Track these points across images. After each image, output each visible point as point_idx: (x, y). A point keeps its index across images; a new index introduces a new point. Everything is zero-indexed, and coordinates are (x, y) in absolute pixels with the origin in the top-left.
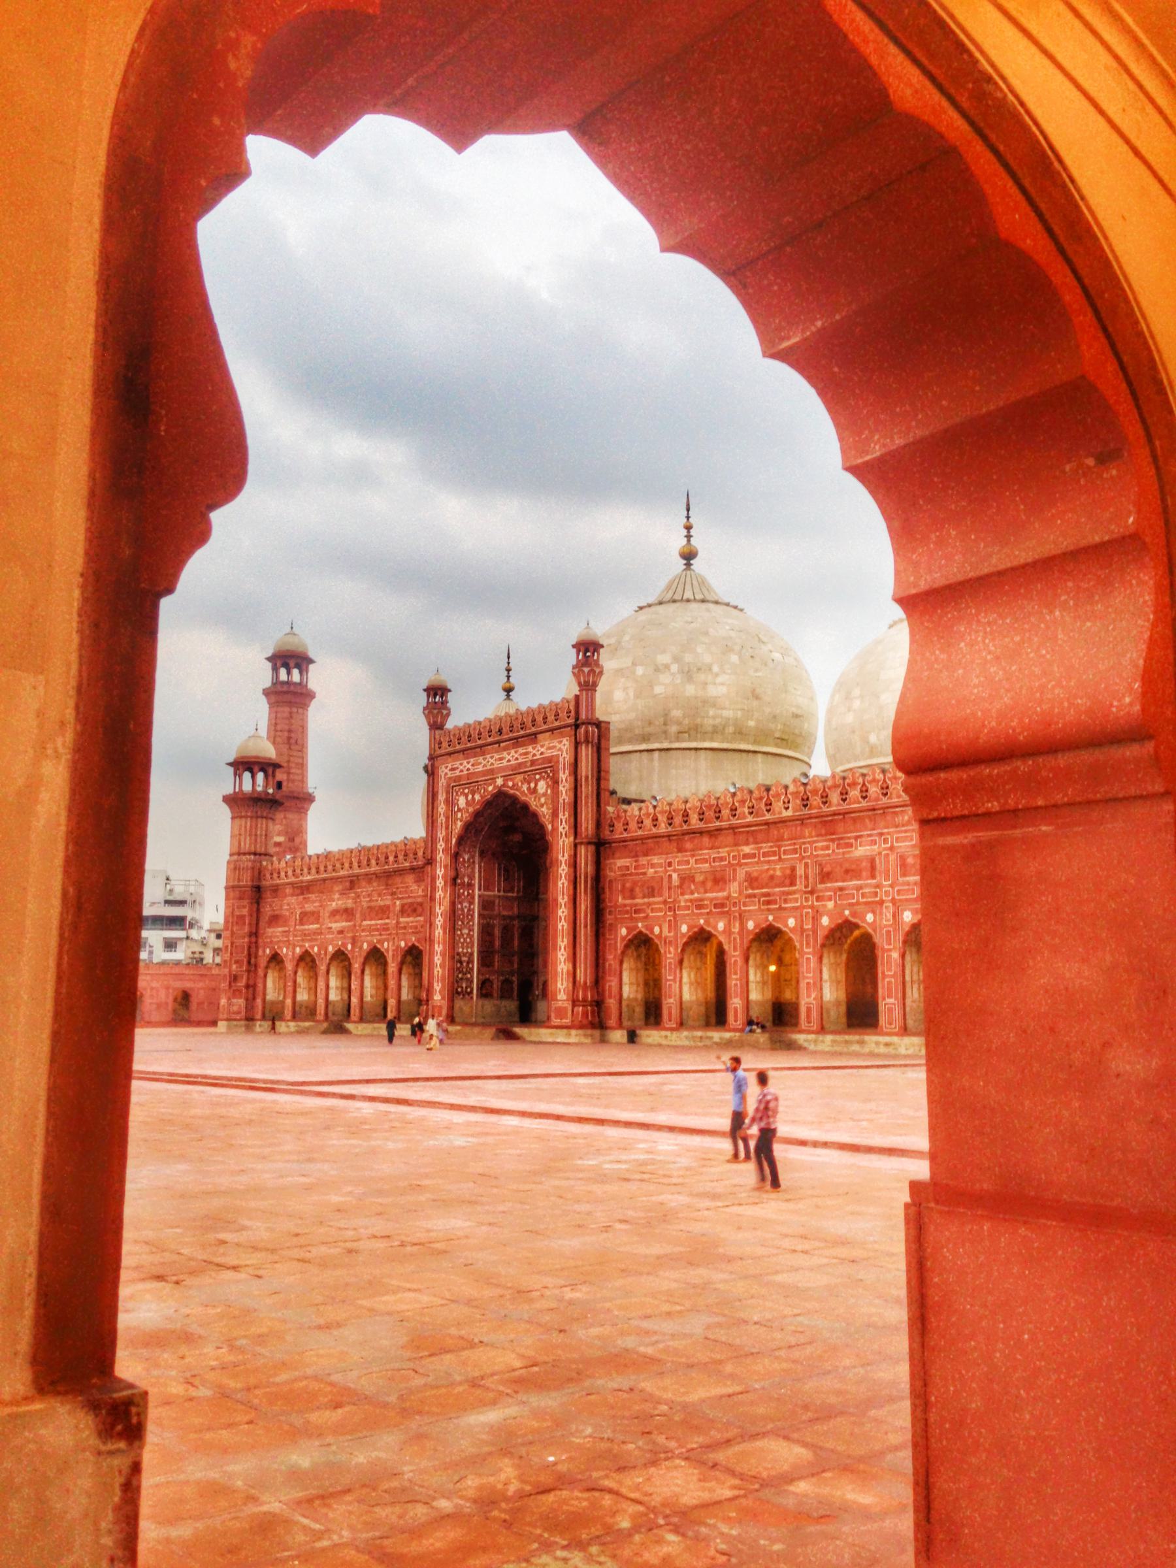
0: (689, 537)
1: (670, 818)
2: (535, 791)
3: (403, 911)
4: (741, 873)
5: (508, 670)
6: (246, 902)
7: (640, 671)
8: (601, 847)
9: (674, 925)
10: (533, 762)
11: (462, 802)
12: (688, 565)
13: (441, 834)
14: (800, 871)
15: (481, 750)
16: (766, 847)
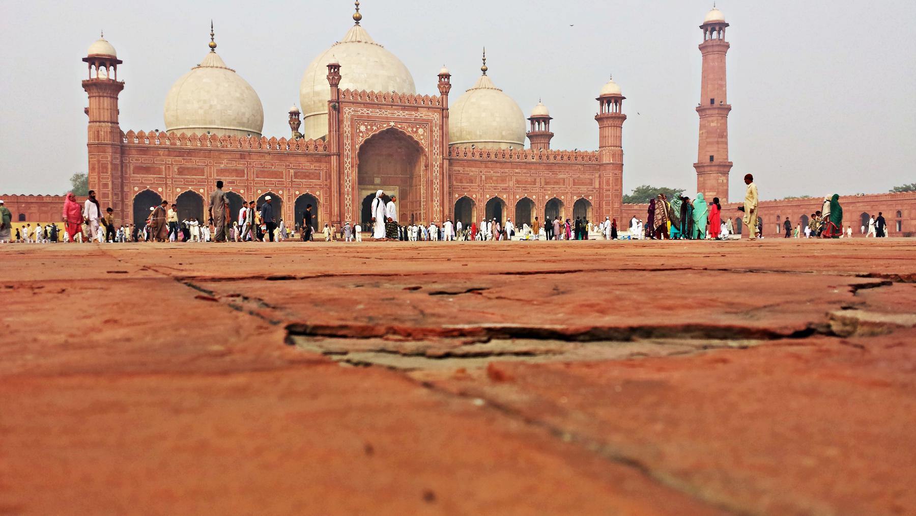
0: (357, 10)
1: (481, 155)
2: (416, 132)
3: (296, 175)
4: (514, 179)
5: (212, 35)
6: (118, 156)
7: (398, 80)
8: (451, 162)
9: (483, 195)
10: (415, 120)
11: (363, 128)
12: (357, 23)
13: (347, 143)
14: (538, 180)
15: (379, 106)
16: (525, 171)
